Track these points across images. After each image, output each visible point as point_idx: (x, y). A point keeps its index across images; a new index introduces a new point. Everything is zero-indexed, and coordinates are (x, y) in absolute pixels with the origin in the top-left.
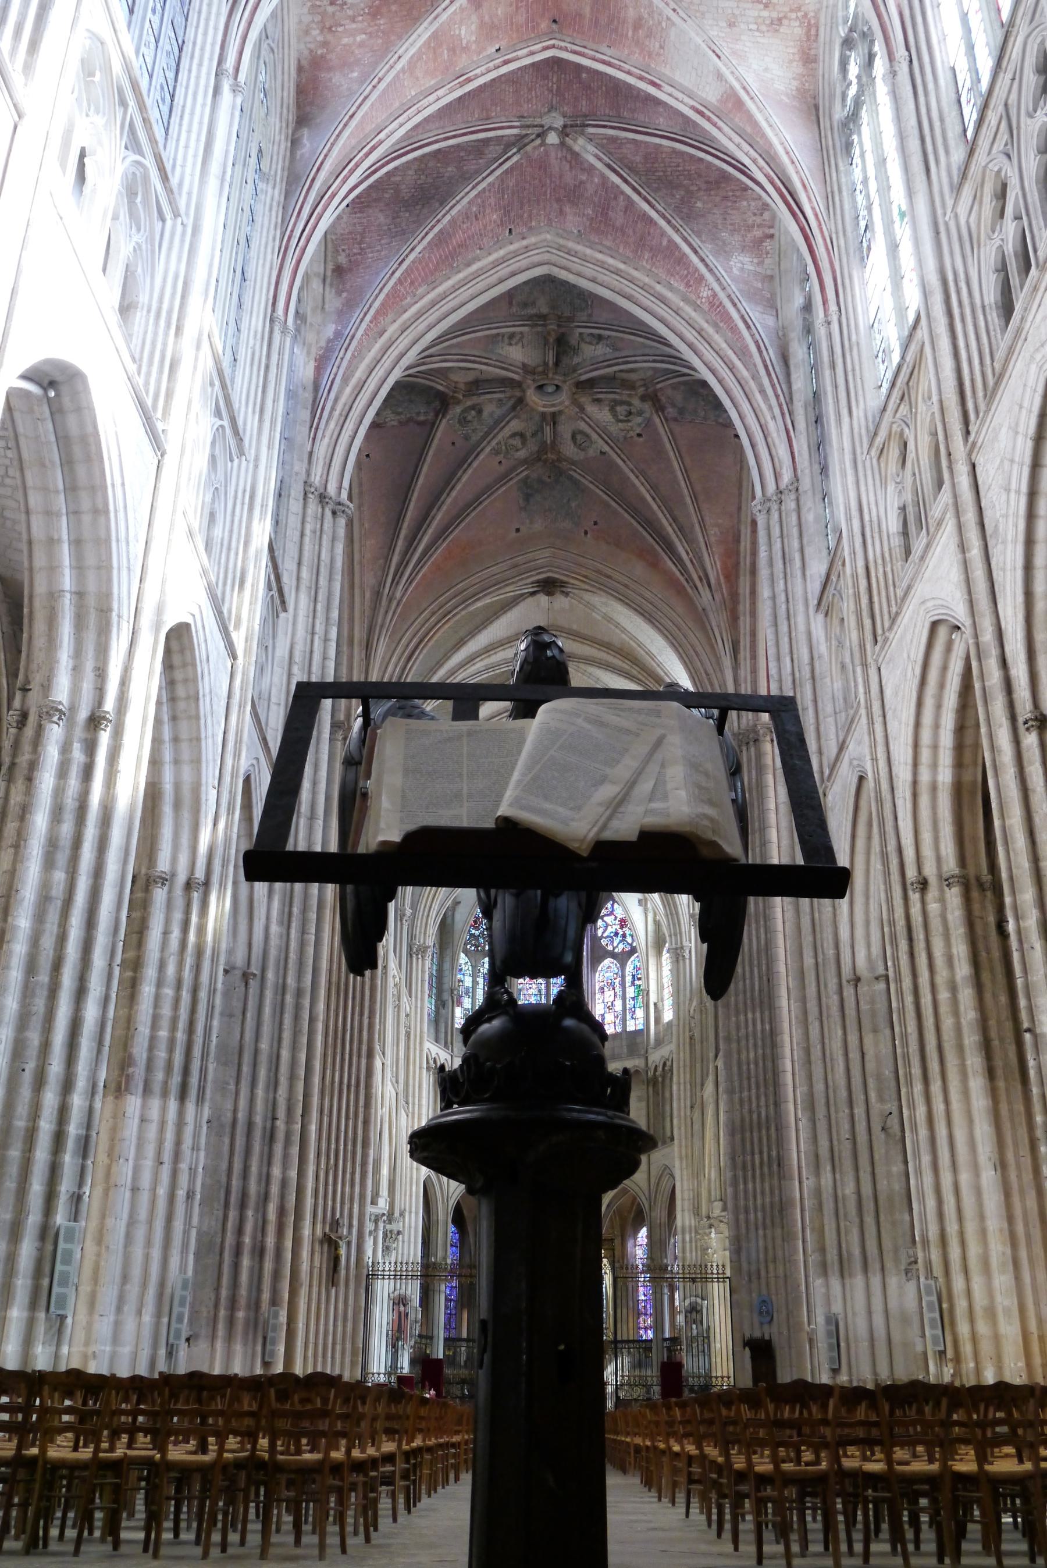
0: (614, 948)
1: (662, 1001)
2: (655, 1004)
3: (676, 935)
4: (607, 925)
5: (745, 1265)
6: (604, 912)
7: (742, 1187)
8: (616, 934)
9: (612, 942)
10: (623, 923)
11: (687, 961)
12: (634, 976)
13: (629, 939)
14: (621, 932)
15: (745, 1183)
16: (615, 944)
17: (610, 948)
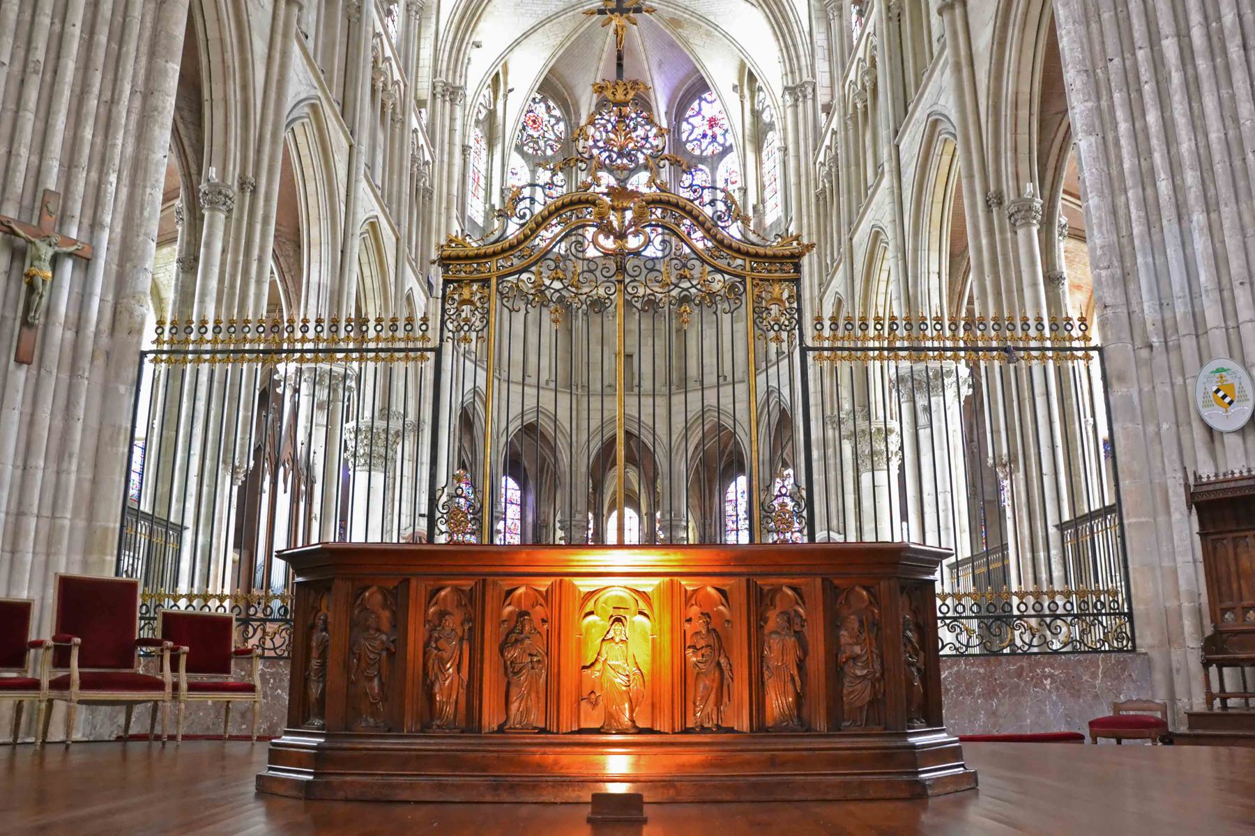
0: (702, 152)
1: (763, 202)
2: (754, 207)
3: (792, 72)
4: (694, 127)
5: (1149, 310)
6: (689, 113)
7: (1123, 127)
8: (705, 136)
9: (700, 146)
10: (712, 123)
11: (810, 103)
12: (726, 180)
13: (720, 139)
14: (709, 133)
15: (1136, 111)
16: (703, 148)
17: (697, 152)
